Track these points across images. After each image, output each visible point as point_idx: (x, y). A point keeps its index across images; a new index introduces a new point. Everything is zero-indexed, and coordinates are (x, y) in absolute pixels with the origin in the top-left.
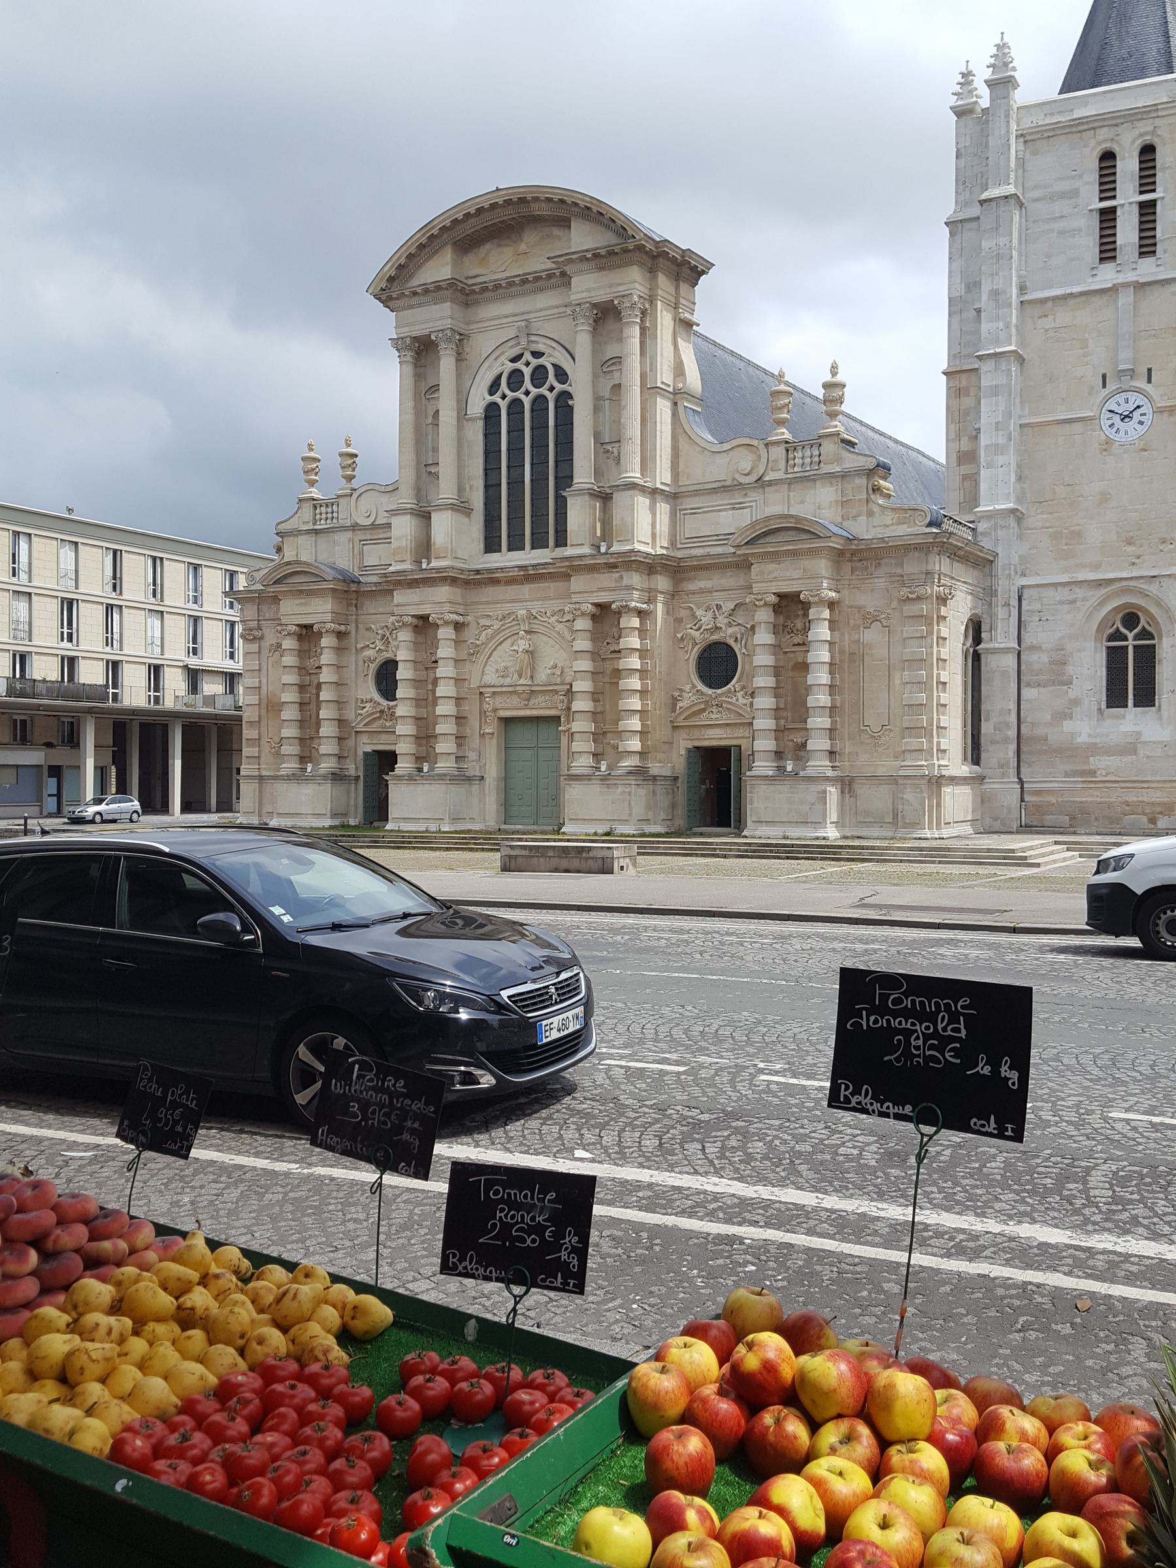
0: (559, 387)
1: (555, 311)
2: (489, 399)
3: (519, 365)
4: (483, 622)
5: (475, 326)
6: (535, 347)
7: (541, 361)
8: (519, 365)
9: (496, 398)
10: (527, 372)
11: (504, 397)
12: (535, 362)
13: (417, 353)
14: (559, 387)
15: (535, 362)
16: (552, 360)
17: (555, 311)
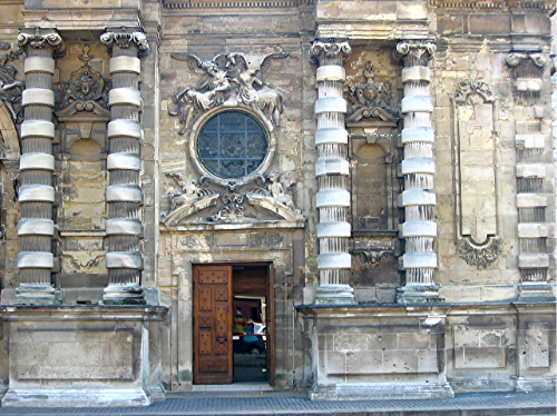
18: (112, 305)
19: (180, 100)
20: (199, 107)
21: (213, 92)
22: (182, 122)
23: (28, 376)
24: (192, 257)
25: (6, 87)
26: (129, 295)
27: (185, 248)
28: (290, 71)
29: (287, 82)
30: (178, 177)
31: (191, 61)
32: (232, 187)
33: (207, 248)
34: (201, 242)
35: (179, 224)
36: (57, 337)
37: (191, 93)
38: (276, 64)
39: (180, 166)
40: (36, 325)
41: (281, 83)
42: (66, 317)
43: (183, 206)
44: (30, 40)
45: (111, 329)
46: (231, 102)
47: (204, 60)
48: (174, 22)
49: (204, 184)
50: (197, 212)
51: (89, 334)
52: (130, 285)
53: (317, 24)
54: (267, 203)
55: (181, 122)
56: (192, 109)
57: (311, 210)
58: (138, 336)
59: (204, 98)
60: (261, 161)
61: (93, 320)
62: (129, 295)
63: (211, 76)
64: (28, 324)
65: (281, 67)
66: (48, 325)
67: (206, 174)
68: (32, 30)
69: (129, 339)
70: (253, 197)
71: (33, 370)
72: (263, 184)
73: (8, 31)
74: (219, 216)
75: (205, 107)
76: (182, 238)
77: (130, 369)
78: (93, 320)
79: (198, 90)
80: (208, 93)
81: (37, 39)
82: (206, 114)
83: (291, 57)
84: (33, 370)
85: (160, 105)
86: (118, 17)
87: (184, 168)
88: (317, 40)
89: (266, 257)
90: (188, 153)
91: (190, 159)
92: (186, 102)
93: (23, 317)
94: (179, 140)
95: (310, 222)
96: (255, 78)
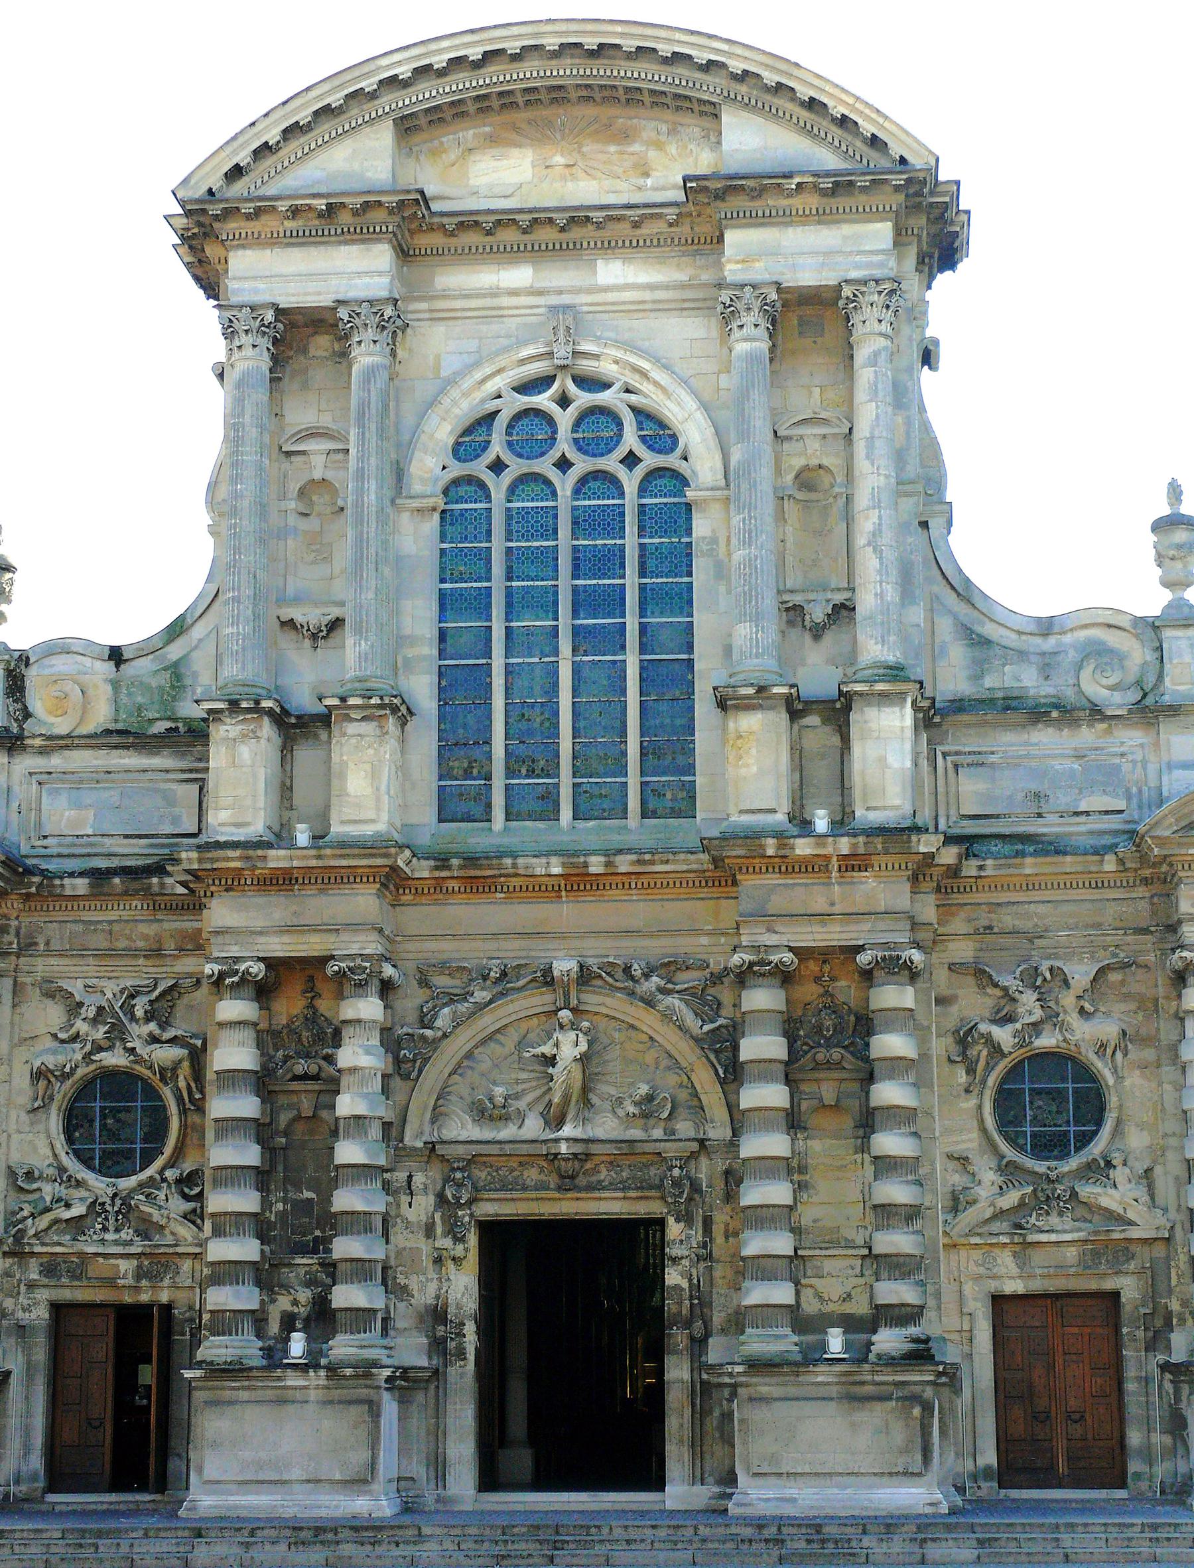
0: (650, 460)
1: (647, 295)
2: (457, 470)
3: (544, 400)
4: (442, 981)
5: (423, 306)
6: (587, 366)
7: (604, 397)
8: (544, 400)
9: (479, 468)
10: (564, 419)
11: (498, 467)
12: (583, 399)
13: (275, 342)
14: (650, 460)
15: (583, 399)
16: (633, 398)
17: (647, 295)
18: (890, 1361)
19: (964, 1038)
20: (996, 1050)
21: (1018, 1026)
22: (971, 1071)
23: (766, 1469)
24: (993, 1286)
25: (706, 1028)
26: (914, 1346)
27: (982, 1270)
28: (1135, 988)
29: (1133, 1006)
30: (966, 1159)
31: (982, 976)
32: (1053, 1175)
33: (1015, 1271)
34: (1006, 1261)
35: (971, 1233)
36: (808, 1408)
37: (983, 1027)
38: (1114, 977)
39: (969, 1141)
40: (776, 1392)
41: (1123, 1007)
42: (820, 1379)
43: (978, 1205)
44: (752, 964)
45: (888, 1398)
46: (1047, 1041)
47: (999, 973)
48: (953, 915)
49: (1009, 1171)
50: (999, 1215)
51: (856, 1404)
52: (913, 1330)
53: (1180, 922)
54: (1109, 1199)
55: (968, 1073)
56: (985, 1053)
57: (1178, 1210)
58: (927, 1408)
59: (1004, 1035)
60: (1096, 1133)
61: (863, 1383)
62: (914, 1346)
63: (1014, 1000)
64: (764, 1390)
65: (1123, 982)
66: (792, 1391)
67: (1010, 1153)
68: (757, 949)
69: (917, 1411)
70: (1086, 1191)
71: (774, 1458)
72: (1101, 1169)
73: (704, 940)
74: (1033, 1220)
75: (1006, 1050)
76: (977, 1255)
77: (919, 1457)
78: (863, 1383)
79: (994, 1021)
80: (1010, 1028)
81: (762, 963)
82: (1007, 1060)
83: (1139, 966)
84: (774, 1458)
85: (940, 1046)
86: (881, 925)
87: (975, 1145)
88: (1182, 947)
89: (1109, 1285)
90: (982, 1121)
91: (984, 1130)
92: (975, 1042)
93: (755, 1380)
94: (967, 1100)
95: (1178, 1229)
96: (1082, 1003)
